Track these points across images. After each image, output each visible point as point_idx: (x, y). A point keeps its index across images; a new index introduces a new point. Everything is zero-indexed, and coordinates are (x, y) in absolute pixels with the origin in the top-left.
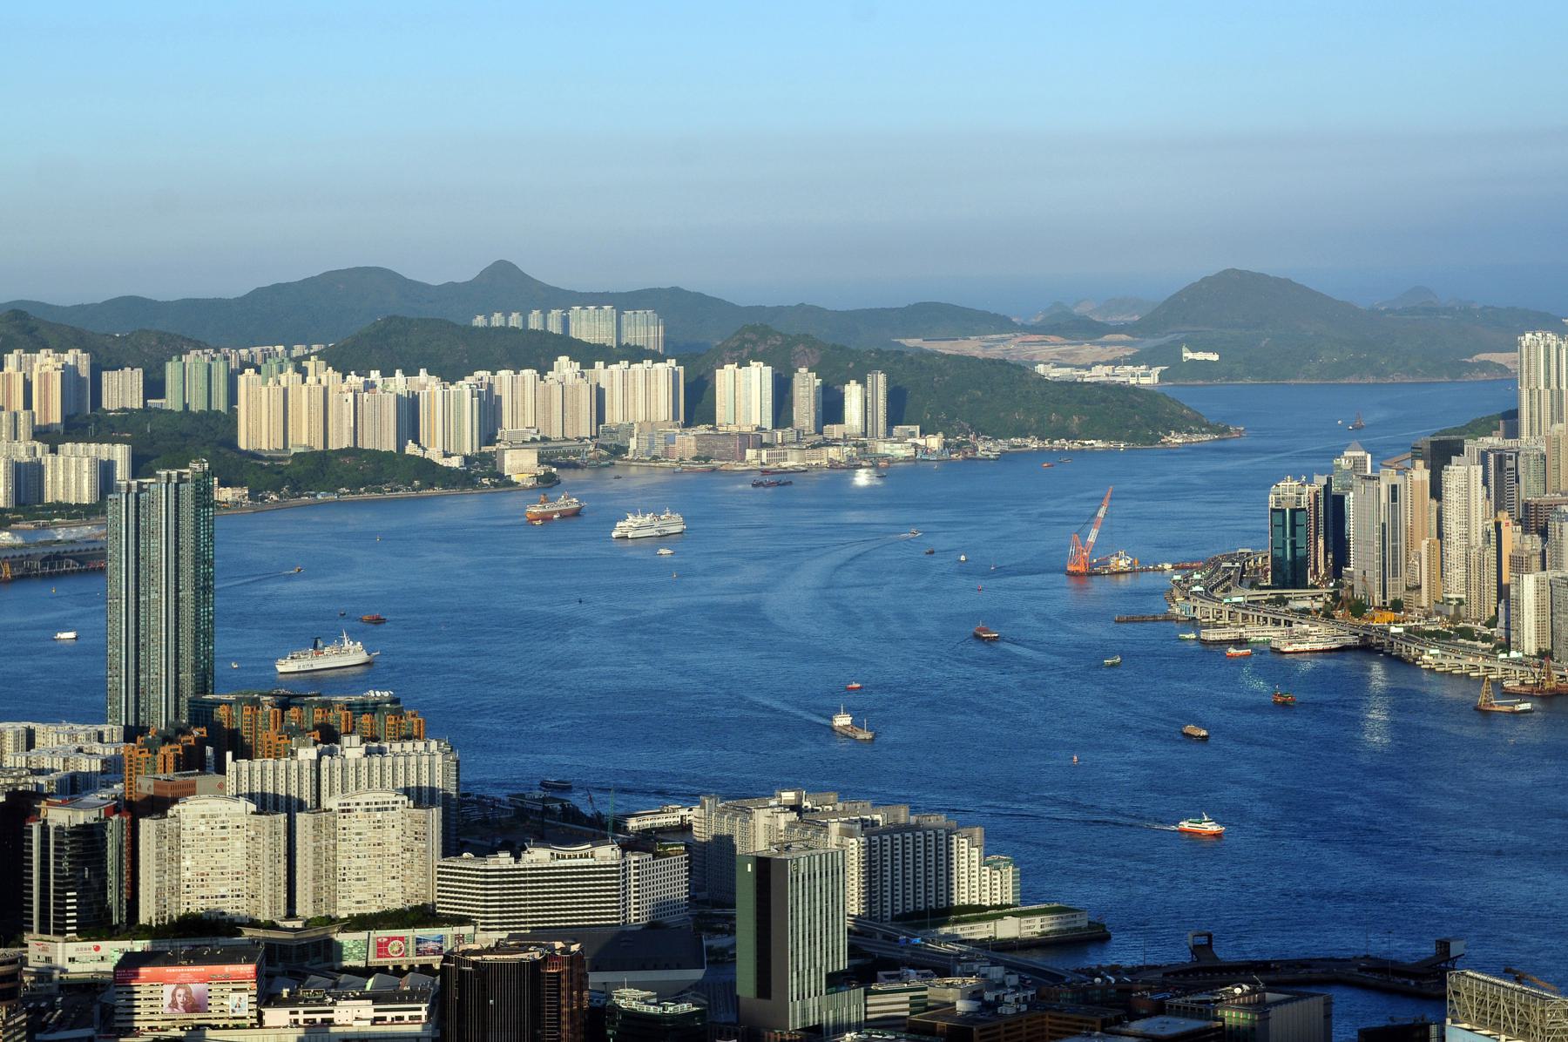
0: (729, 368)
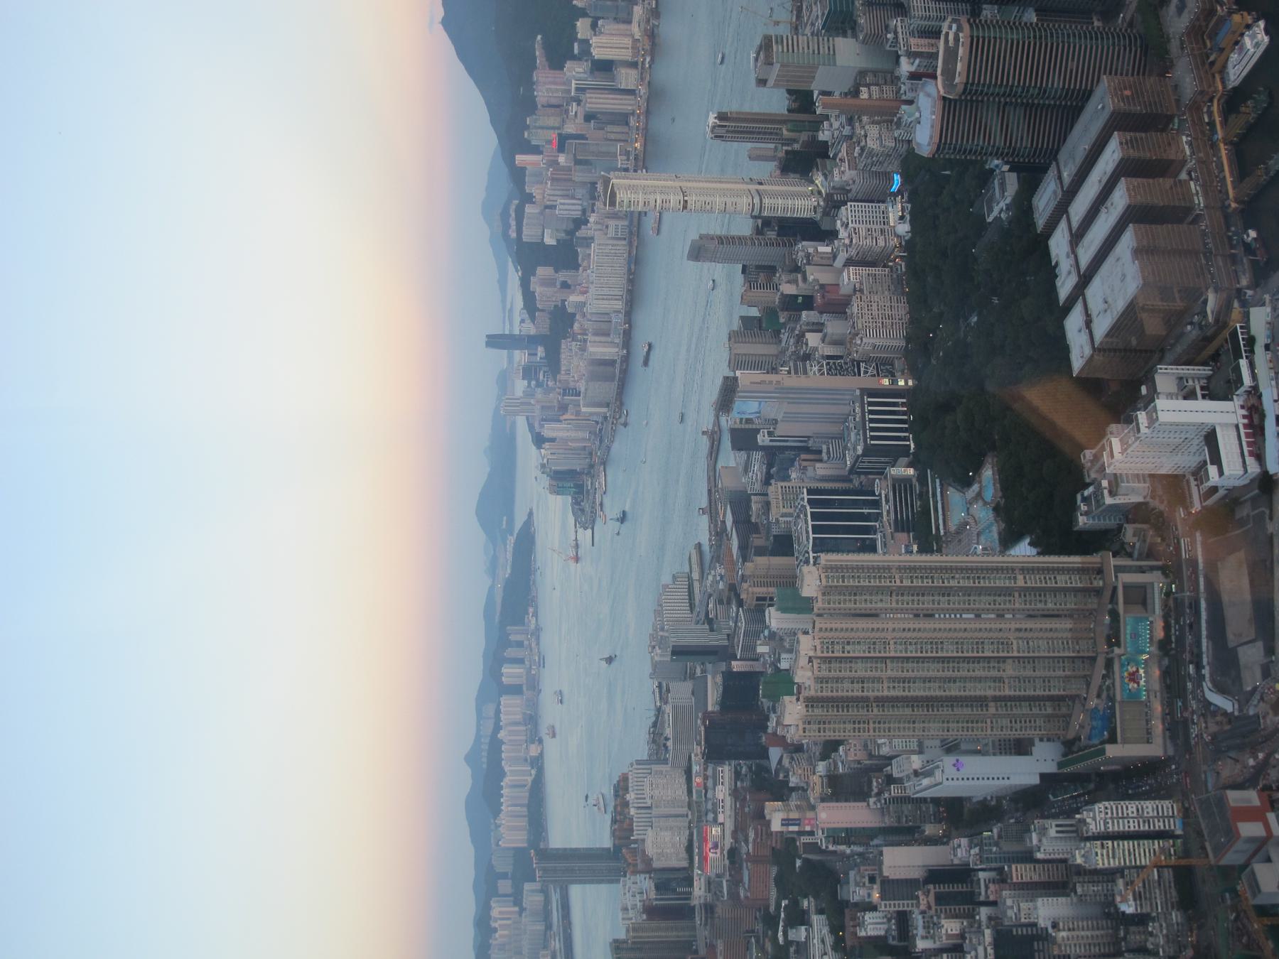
0: (503, 679)
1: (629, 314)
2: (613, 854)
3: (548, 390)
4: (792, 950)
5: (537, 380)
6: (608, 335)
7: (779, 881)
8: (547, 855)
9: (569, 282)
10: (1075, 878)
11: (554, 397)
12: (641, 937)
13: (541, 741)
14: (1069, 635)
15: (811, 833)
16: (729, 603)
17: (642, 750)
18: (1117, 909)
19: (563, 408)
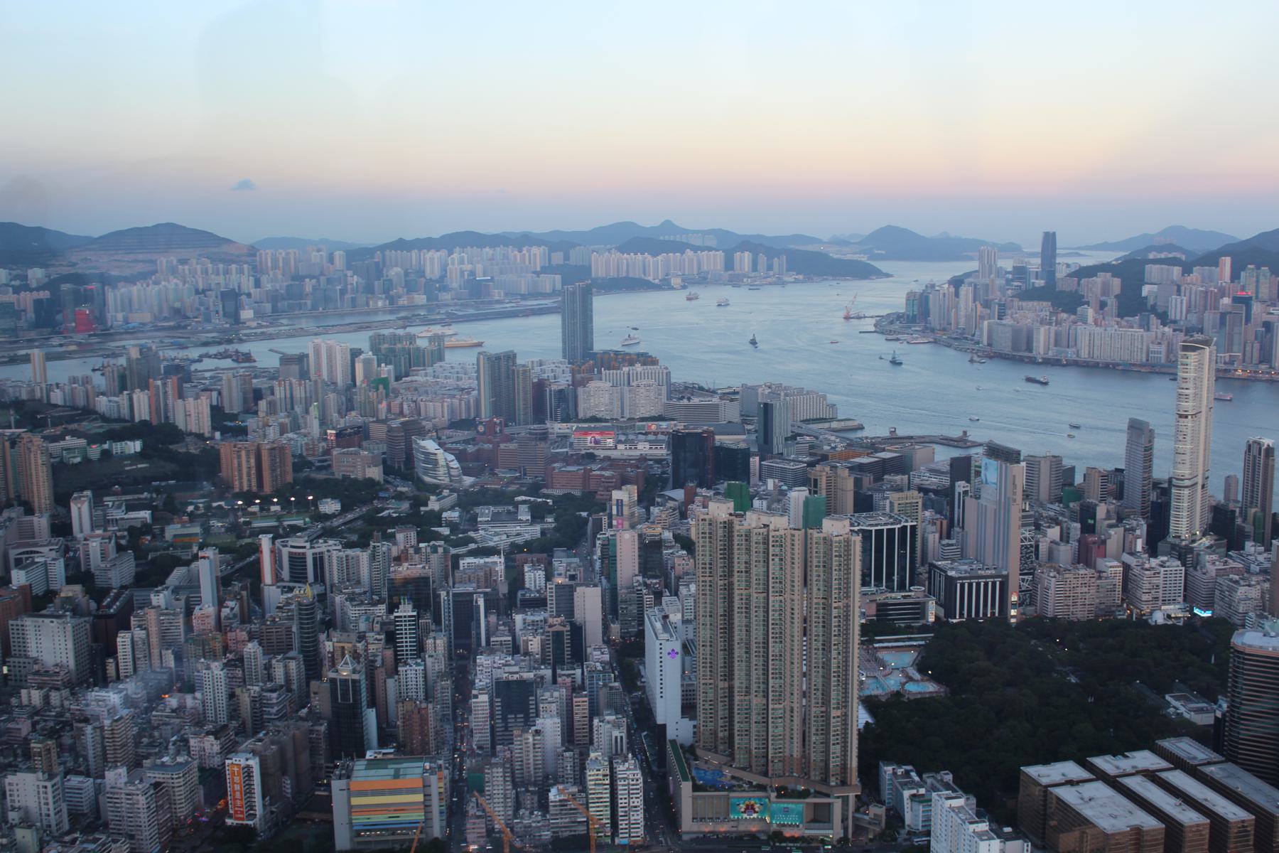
1: (1075, 364)
2: (588, 352)
3: (1003, 290)
4: (510, 508)
5: (1012, 280)
6: (1056, 345)
7: (568, 497)
8: (586, 295)
9: (1106, 309)
10: (577, 751)
11: (996, 296)
12: (518, 377)
13: (684, 287)
14: (787, 754)
15: (610, 526)
16: (811, 454)
17: (678, 377)
18: (553, 785)
19: (987, 304)
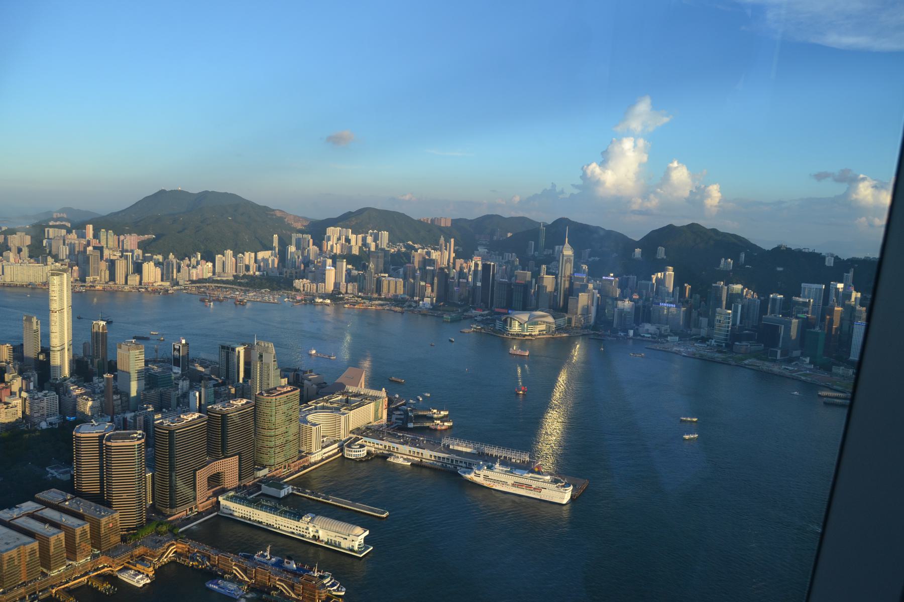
9: (21, 253)
